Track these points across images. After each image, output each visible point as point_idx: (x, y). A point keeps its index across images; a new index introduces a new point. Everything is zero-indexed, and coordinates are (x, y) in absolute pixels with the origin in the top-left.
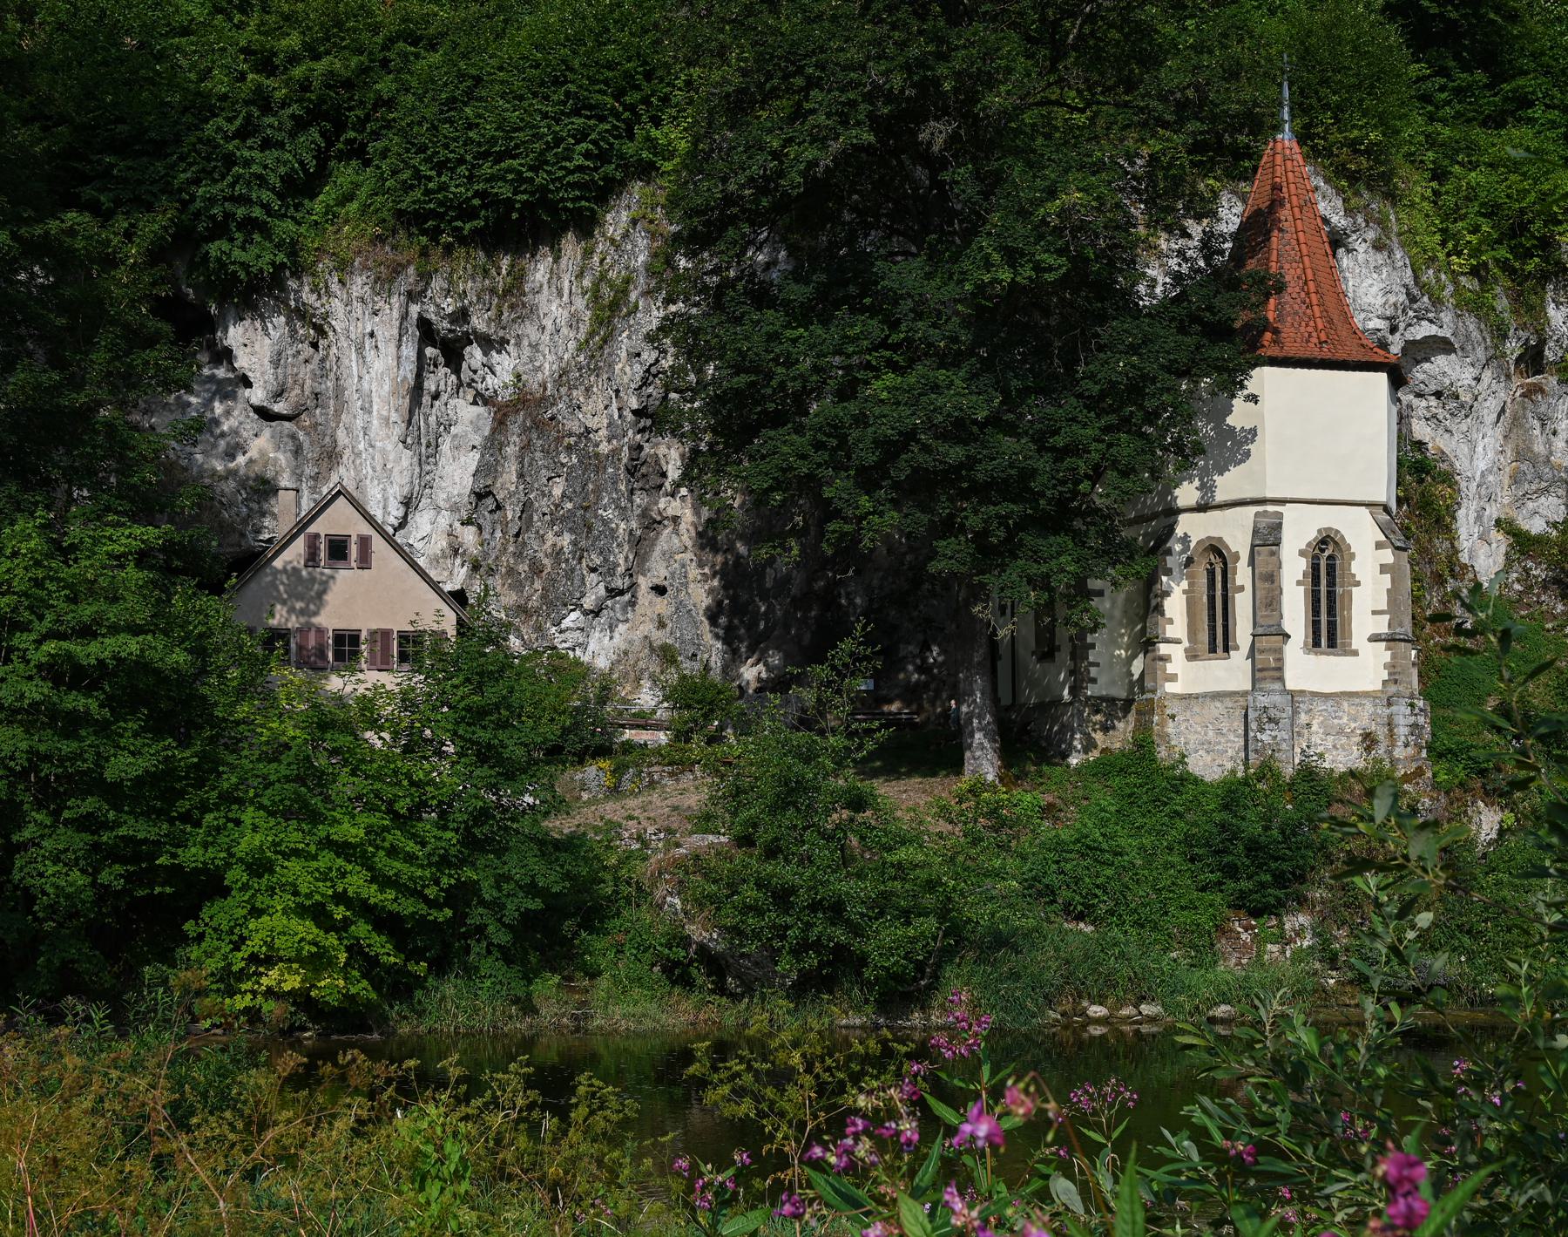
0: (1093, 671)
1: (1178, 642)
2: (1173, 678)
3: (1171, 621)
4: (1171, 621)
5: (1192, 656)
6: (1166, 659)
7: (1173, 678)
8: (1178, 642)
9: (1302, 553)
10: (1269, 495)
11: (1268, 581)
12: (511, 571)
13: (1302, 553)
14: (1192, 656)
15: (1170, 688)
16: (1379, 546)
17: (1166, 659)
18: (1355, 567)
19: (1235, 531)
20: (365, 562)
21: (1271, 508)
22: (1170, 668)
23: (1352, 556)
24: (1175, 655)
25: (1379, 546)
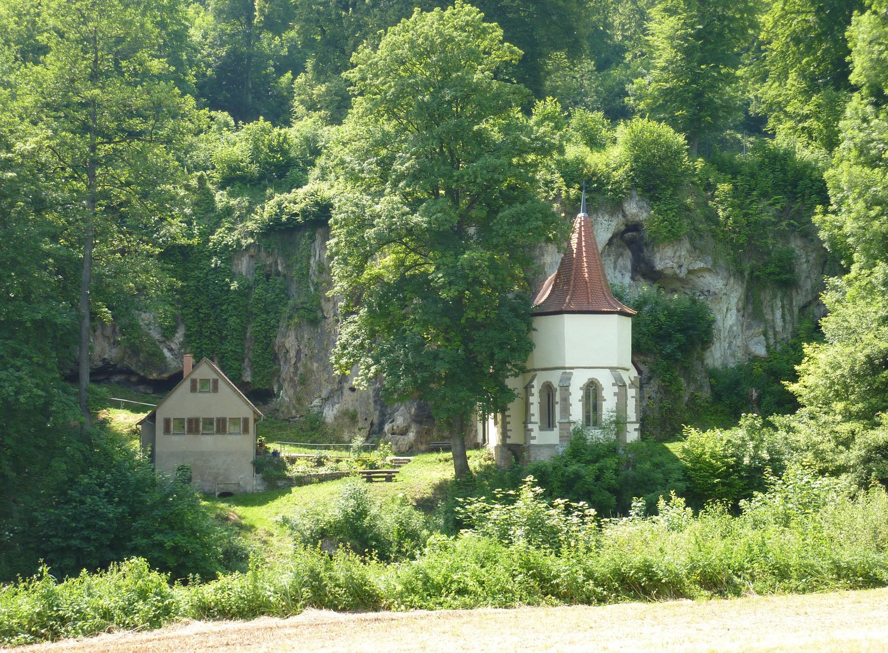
0: (509, 433)
1: (536, 423)
2: (534, 438)
3: (533, 415)
4: (533, 415)
5: (541, 429)
6: (532, 430)
7: (534, 438)
8: (536, 423)
9: (581, 389)
10: (567, 366)
11: (565, 400)
12: (292, 380)
13: (581, 389)
14: (541, 429)
15: (533, 442)
16: (614, 385)
17: (532, 430)
18: (604, 394)
19: (554, 378)
20: (215, 389)
21: (568, 371)
22: (533, 434)
23: (603, 389)
24: (535, 428)
25: (614, 385)
